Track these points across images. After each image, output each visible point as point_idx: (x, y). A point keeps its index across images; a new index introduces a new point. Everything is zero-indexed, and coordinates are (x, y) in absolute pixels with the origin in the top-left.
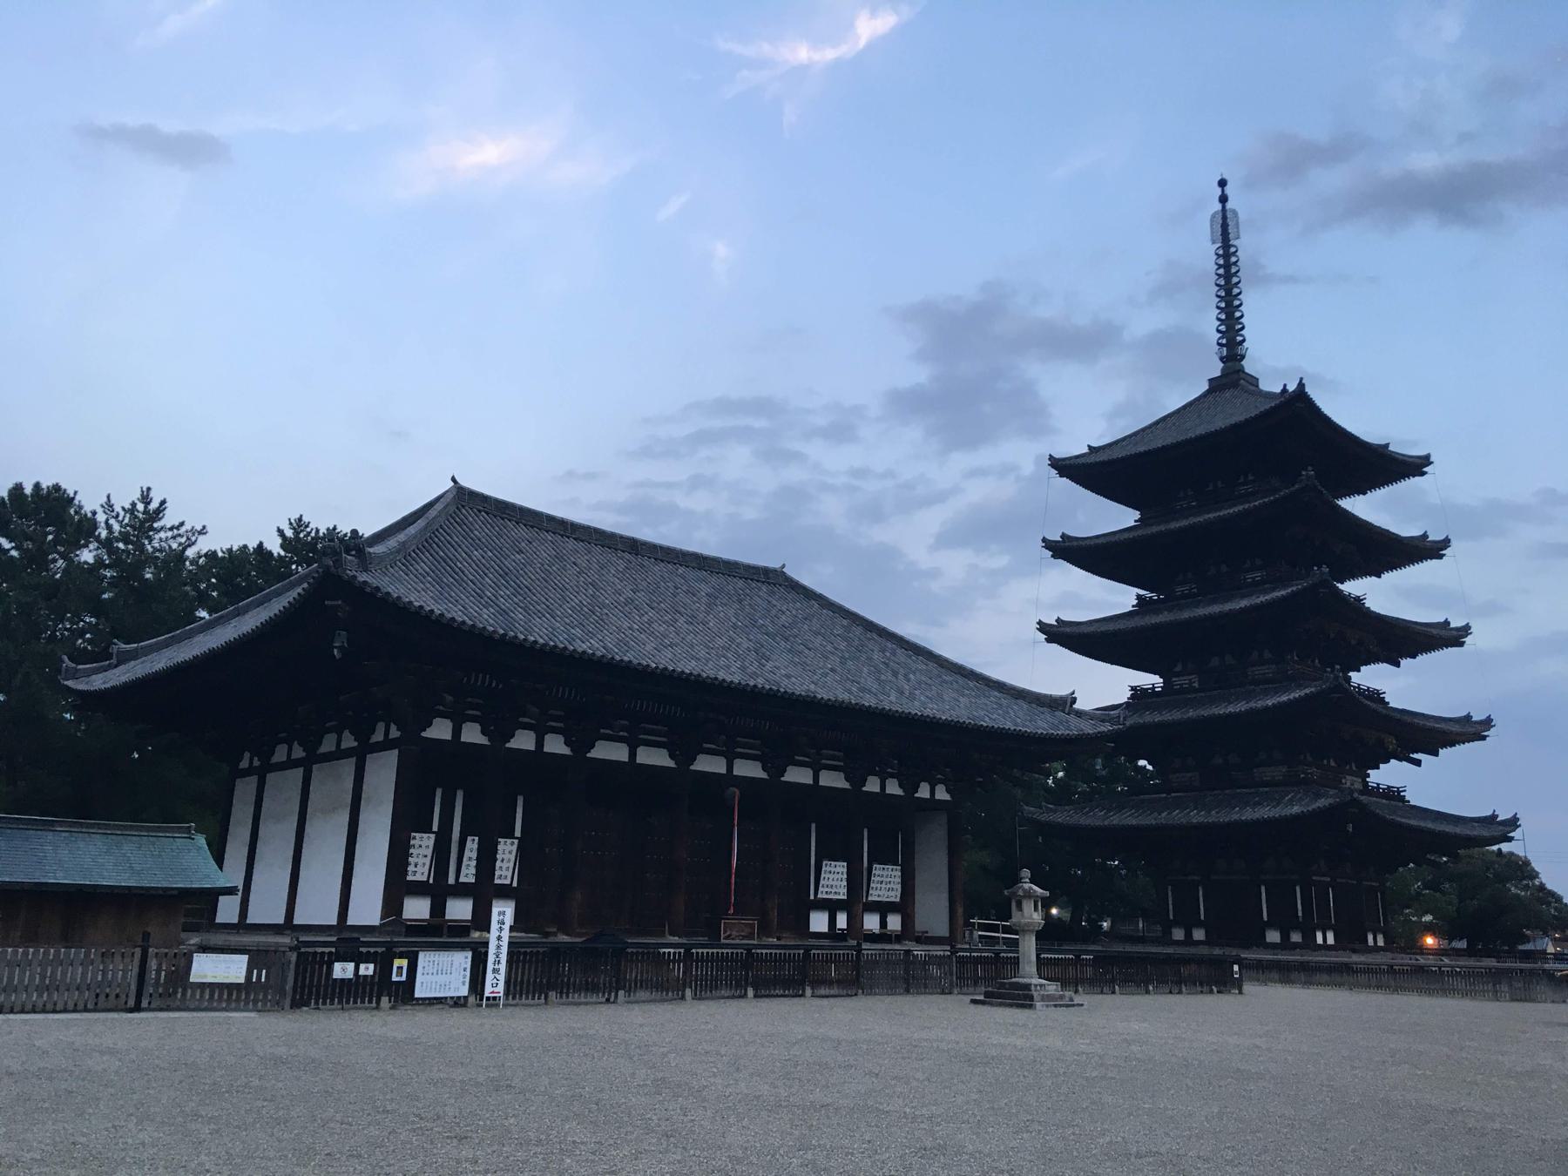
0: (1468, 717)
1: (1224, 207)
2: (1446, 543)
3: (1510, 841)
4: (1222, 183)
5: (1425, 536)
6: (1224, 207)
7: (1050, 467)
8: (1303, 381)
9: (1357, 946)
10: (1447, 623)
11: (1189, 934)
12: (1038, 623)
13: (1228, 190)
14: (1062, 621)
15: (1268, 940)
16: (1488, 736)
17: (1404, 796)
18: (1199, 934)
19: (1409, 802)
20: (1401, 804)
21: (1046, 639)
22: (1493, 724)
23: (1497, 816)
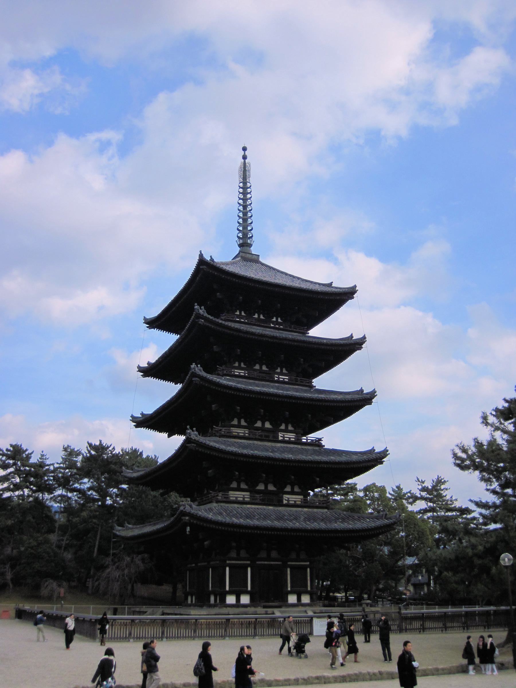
0: (373, 450)
1: (245, 163)
2: (364, 338)
4: (244, 149)
5: (352, 336)
6: (245, 163)
10: (362, 391)
20: (326, 510)
21: (134, 426)
22: (388, 453)
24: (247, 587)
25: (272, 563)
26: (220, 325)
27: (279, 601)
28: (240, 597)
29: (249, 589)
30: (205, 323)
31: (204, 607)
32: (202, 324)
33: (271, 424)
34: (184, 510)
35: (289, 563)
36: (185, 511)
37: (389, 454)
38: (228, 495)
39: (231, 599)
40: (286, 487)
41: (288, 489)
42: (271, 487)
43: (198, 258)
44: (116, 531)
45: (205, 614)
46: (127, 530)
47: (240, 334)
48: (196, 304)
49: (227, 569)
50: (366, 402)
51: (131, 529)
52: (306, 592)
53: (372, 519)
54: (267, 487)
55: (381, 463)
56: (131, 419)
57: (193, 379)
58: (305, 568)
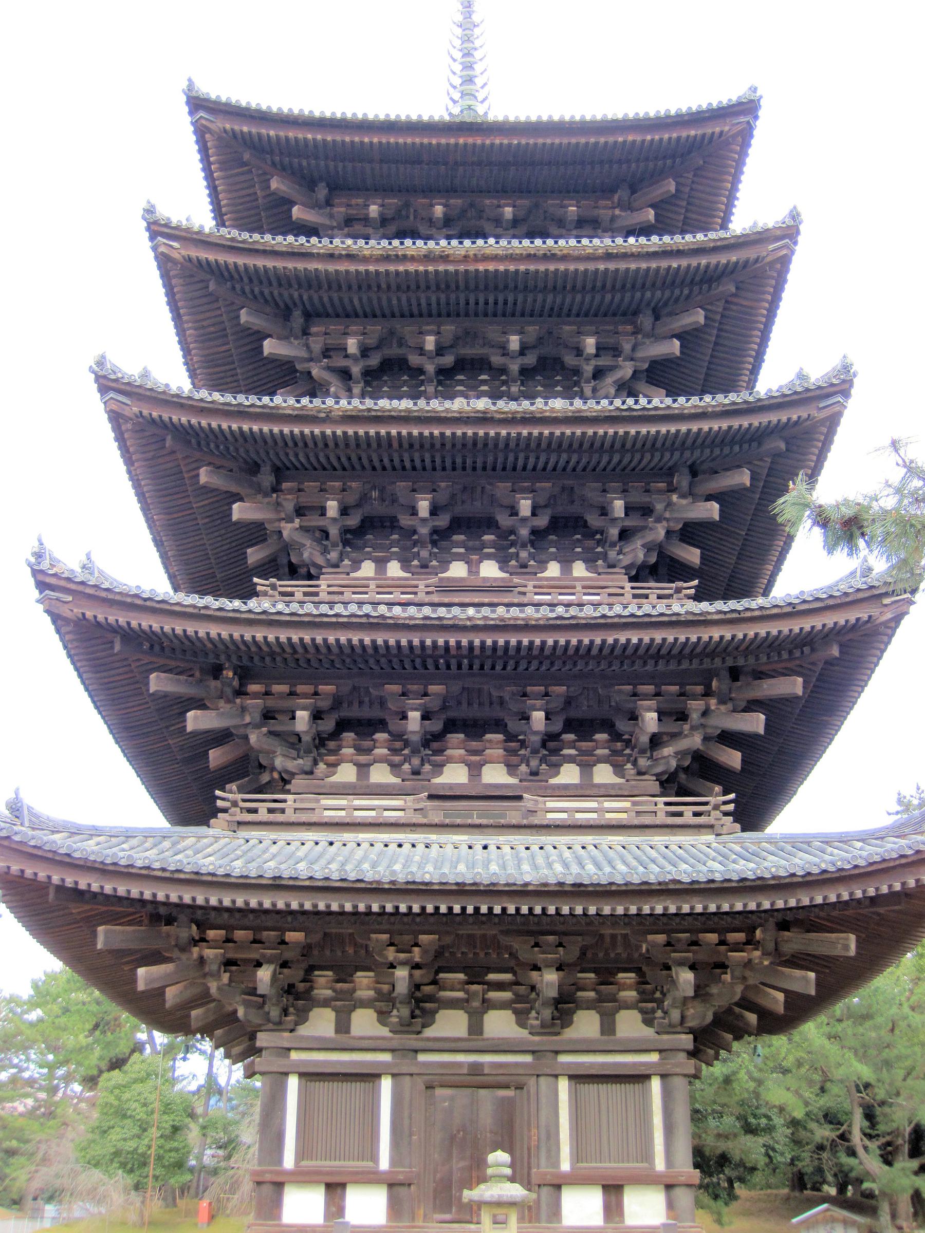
2: (795, 215)
10: (801, 376)
20: (711, 838)
24: (375, 1158)
28: (343, 1197)
29: (384, 1163)
30: (184, 252)
32: (175, 255)
33: (501, 569)
38: (285, 801)
40: (558, 773)
43: (185, 99)
47: (312, 266)
49: (293, 1082)
52: (647, 1179)
53: (882, 838)
54: (480, 775)
58: (640, 1078)
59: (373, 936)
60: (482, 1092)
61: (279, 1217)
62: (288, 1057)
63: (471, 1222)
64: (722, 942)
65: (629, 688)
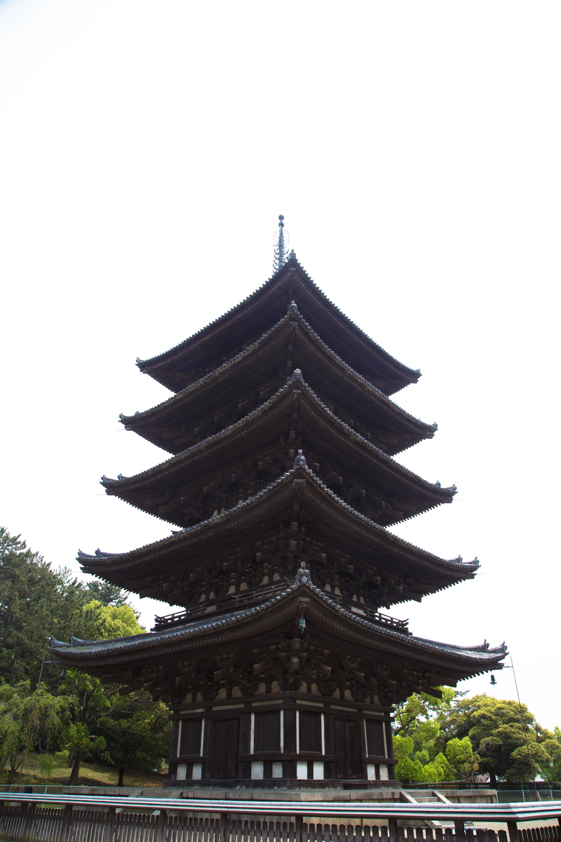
3: (501, 668)
4: (281, 218)
7: (137, 366)
8: (294, 252)
9: (356, 781)
11: (189, 774)
12: (102, 478)
13: (283, 221)
14: (122, 477)
15: (253, 777)
16: (475, 574)
17: (407, 628)
18: (197, 773)
19: (411, 634)
22: (479, 564)
23: (488, 645)
24: (321, 750)
25: (347, 709)
26: (313, 342)
27: (358, 778)
29: (323, 753)
31: (238, 787)
34: (307, 585)
35: (365, 712)
36: (308, 587)
37: (480, 566)
39: (302, 772)
41: (355, 598)
42: (337, 592)
44: (54, 647)
45: (321, 799)
46: (74, 647)
48: (293, 302)
50: (446, 499)
51: (82, 645)
55: (472, 577)
56: (102, 481)
57: (294, 391)
59: (346, 656)
60: (346, 723)
61: (296, 776)
62: (296, 702)
63: (346, 779)
64: (417, 676)
65: (388, 574)
